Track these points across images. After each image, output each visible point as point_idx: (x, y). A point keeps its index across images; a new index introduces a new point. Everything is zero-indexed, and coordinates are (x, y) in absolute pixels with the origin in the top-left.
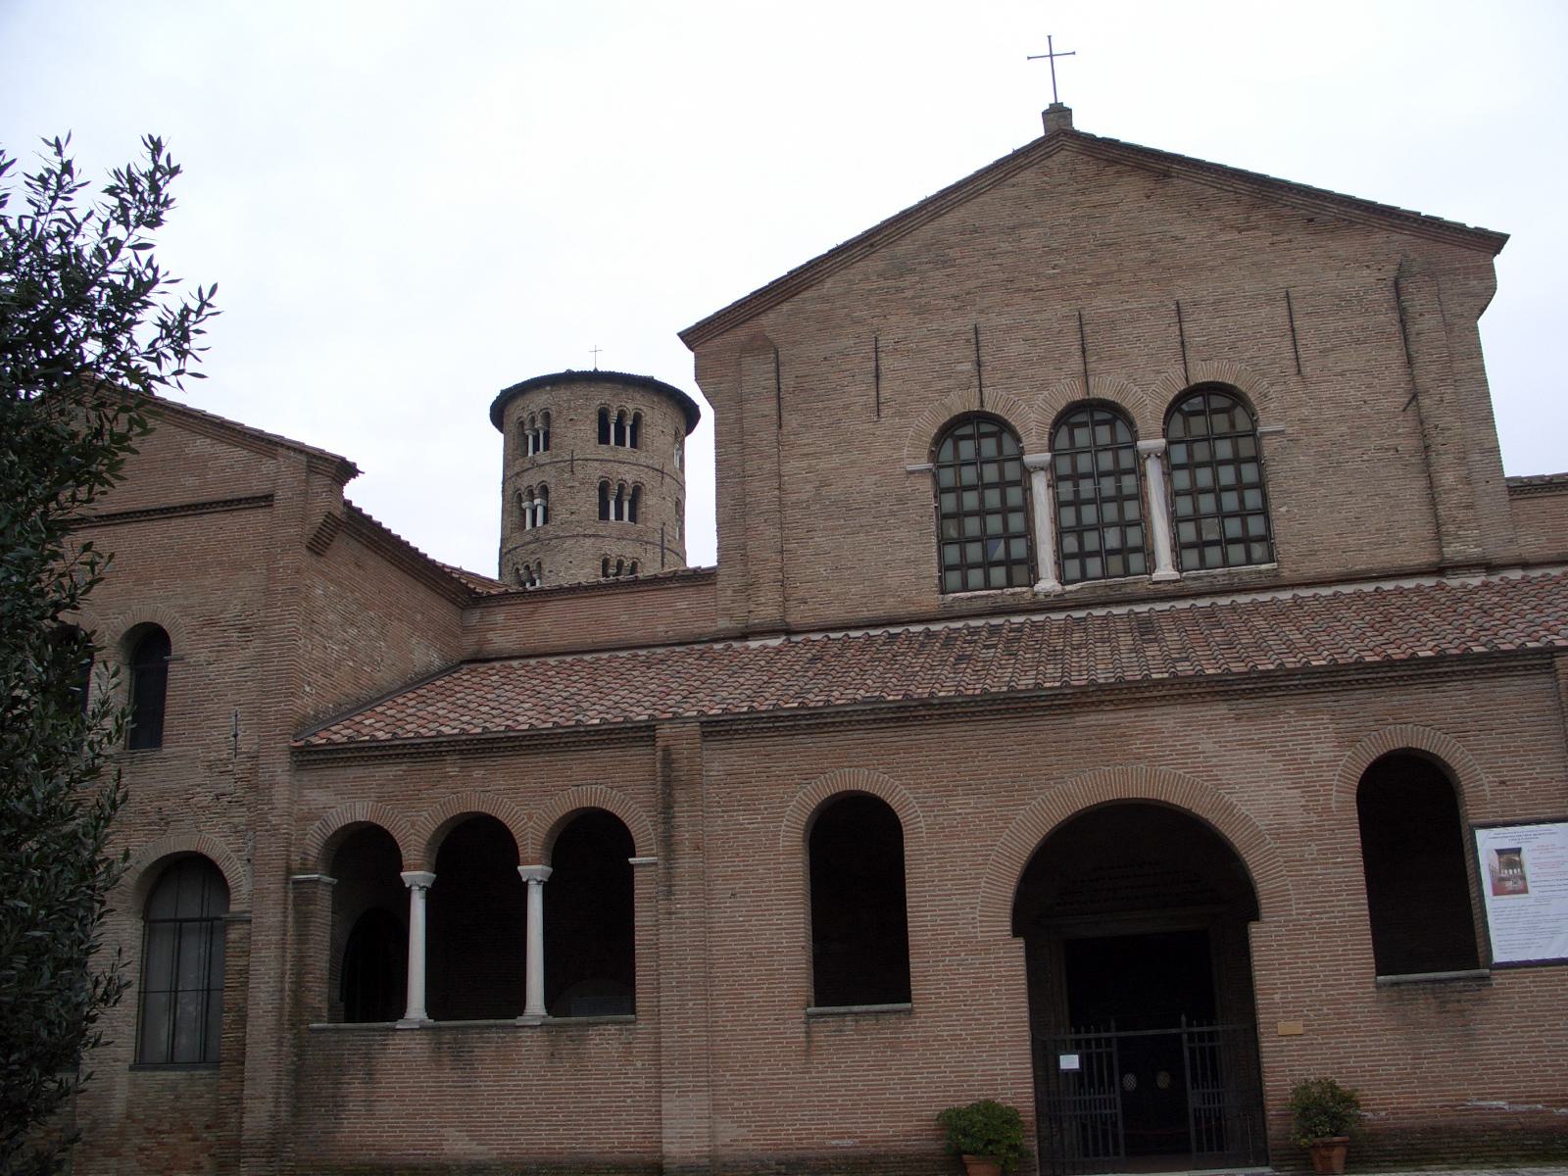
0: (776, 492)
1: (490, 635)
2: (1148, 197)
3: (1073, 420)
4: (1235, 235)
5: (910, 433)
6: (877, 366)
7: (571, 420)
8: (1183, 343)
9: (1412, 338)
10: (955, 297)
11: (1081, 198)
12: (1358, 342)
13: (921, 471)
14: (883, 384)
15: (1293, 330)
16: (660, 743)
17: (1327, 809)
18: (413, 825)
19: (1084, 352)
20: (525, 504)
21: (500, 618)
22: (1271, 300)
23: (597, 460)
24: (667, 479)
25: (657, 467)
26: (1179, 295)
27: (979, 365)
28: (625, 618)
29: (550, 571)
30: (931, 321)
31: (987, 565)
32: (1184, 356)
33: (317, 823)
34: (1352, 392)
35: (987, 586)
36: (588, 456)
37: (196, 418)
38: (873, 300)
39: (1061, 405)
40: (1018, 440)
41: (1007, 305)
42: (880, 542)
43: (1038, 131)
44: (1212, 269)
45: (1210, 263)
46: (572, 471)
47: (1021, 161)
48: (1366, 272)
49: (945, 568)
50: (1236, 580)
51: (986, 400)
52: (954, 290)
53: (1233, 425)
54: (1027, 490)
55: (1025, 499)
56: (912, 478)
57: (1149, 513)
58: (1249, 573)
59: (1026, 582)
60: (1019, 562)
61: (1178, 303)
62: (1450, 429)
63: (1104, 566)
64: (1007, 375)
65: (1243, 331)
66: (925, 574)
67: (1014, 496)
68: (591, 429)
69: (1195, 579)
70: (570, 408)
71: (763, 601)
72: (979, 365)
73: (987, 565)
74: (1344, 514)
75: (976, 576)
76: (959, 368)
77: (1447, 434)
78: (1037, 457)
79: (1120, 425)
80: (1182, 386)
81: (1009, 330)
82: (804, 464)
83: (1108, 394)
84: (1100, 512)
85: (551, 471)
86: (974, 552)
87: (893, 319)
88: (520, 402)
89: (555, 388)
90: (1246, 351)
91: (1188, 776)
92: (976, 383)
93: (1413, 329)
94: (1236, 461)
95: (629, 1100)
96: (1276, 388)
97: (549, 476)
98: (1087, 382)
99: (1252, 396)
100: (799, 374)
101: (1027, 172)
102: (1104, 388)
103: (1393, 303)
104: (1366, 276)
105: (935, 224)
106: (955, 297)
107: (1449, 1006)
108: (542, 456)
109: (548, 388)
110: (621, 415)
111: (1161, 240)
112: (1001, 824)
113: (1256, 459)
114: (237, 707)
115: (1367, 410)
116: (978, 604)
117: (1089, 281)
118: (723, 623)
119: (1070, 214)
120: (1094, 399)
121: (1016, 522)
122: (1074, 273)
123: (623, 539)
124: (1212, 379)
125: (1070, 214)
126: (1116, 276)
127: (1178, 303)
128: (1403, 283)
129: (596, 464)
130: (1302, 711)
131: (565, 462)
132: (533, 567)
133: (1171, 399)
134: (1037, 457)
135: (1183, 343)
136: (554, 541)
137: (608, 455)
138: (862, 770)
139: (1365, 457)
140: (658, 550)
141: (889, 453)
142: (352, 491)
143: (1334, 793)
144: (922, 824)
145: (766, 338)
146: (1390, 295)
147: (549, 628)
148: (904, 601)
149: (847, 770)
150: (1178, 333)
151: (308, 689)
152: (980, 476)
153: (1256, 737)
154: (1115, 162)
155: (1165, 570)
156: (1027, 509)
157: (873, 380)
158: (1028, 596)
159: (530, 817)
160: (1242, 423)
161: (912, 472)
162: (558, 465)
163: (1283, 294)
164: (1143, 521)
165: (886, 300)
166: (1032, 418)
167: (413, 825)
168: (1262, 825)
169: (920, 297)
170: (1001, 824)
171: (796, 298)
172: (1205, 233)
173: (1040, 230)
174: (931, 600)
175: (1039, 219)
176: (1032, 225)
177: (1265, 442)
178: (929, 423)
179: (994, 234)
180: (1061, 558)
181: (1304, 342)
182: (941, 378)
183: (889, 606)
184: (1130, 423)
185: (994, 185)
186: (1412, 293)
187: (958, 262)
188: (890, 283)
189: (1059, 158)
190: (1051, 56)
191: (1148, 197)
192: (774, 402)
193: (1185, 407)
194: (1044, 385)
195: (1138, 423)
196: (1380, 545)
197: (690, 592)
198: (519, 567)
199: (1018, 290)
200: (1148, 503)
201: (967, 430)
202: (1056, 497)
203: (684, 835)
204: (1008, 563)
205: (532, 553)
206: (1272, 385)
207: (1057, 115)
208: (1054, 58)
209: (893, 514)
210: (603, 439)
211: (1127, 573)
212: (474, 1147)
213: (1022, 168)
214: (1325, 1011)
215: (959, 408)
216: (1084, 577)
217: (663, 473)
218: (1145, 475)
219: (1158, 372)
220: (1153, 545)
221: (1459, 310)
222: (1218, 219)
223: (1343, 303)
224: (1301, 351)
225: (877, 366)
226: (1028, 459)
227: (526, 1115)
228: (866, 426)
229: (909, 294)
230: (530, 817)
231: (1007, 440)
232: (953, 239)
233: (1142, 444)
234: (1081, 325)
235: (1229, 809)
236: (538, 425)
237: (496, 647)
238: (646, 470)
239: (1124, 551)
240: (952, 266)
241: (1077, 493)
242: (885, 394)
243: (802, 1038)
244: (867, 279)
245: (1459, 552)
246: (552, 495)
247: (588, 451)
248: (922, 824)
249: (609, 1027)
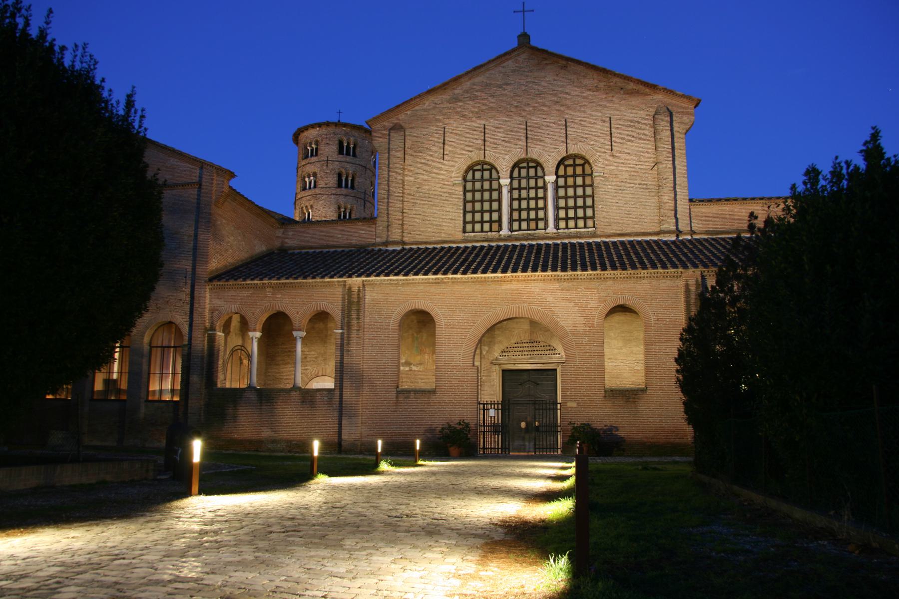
0: (401, 189)
1: (286, 240)
2: (557, 75)
3: (521, 165)
4: (591, 93)
5: (456, 168)
6: (444, 140)
7: (327, 144)
8: (566, 137)
9: (658, 140)
10: (477, 113)
11: (530, 74)
12: (636, 140)
13: (459, 184)
14: (446, 147)
15: (611, 134)
16: (347, 287)
17: (593, 325)
18: (253, 314)
19: (527, 138)
20: (307, 179)
21: (290, 234)
22: (603, 121)
24: (368, 171)
25: (363, 165)
26: (566, 117)
27: (485, 141)
28: (340, 236)
29: (316, 209)
30: (466, 122)
31: (482, 222)
32: (566, 142)
33: (217, 312)
34: (632, 161)
35: (482, 231)
36: (334, 160)
37: (171, 150)
38: (444, 112)
39: (516, 160)
40: (498, 173)
41: (497, 117)
42: (441, 210)
43: (516, 45)
44: (581, 107)
45: (580, 104)
46: (327, 166)
47: (507, 57)
48: (642, 112)
49: (465, 222)
50: (579, 234)
51: (486, 156)
52: (476, 110)
53: (583, 171)
54: (500, 193)
55: (499, 197)
56: (455, 186)
57: (547, 205)
58: (585, 232)
59: (497, 230)
60: (495, 221)
61: (566, 120)
62: (668, 178)
63: (528, 225)
64: (495, 146)
65: (591, 133)
66: (458, 225)
67: (495, 195)
68: (334, 148)
69: (563, 233)
70: (327, 138)
71: (394, 231)
72: (485, 141)
73: (482, 222)
74: (624, 210)
75: (478, 227)
76: (477, 142)
77: (667, 180)
78: (505, 182)
79: (539, 168)
80: (564, 154)
81: (497, 128)
82: (413, 178)
83: (535, 157)
84: (528, 203)
85: (318, 165)
86: (478, 217)
87: (452, 121)
88: (306, 134)
89: (321, 129)
90: (591, 141)
91: (542, 310)
92: (483, 148)
93: (658, 137)
94: (584, 186)
95: (330, 419)
96: (602, 157)
98: (527, 151)
99: (591, 161)
100: (414, 141)
101: (510, 61)
102: (534, 153)
103: (652, 125)
104: (642, 114)
105: (471, 81)
106: (477, 113)
107: (631, 400)
108: (314, 159)
110: (348, 144)
111: (561, 94)
112: (472, 324)
113: (592, 185)
114: (186, 267)
115: (637, 168)
116: (478, 238)
117: (531, 109)
118: (378, 240)
119: (525, 81)
120: (529, 158)
121: (495, 205)
122: (525, 106)
123: (348, 196)
124: (576, 152)
125: (525, 81)
126: (542, 108)
127: (566, 120)
128: (656, 116)
129: (337, 163)
130: (587, 289)
131: (324, 161)
133: (559, 159)
134: (505, 182)
135: (566, 137)
136: (319, 195)
137: (344, 159)
138: (422, 301)
139: (634, 188)
140: (362, 201)
141: (447, 175)
142: (234, 183)
143: (596, 319)
144: (443, 322)
145: (401, 125)
146: (651, 121)
147: (309, 239)
148: (449, 235)
149: (416, 301)
150: (565, 132)
151: (214, 260)
152: (482, 186)
153: (569, 297)
154: (546, 59)
155: (551, 229)
156: (499, 200)
157: (442, 145)
158: (497, 236)
159: (298, 313)
160: (588, 171)
161: (456, 184)
162: (321, 163)
163: (608, 119)
164: (545, 208)
165: (449, 112)
166: (504, 165)
167: (253, 314)
168: (568, 329)
169: (463, 112)
170: (472, 324)
171: (413, 109)
172: (579, 92)
173: (512, 87)
174: (460, 236)
175: (513, 82)
176: (511, 84)
177: (595, 179)
178: (462, 163)
179: (494, 87)
180: (511, 221)
181: (615, 139)
182: (469, 146)
183: (443, 236)
184: (543, 169)
185: (496, 66)
186: (659, 122)
187: (479, 98)
188: (452, 105)
189: (524, 56)
190: (524, 11)
191: (557, 75)
192: (402, 153)
193: (567, 162)
194: (508, 152)
195: (546, 170)
196: (637, 223)
197: (366, 227)
199: (502, 111)
200: (547, 201)
201: (479, 167)
202: (511, 196)
203: (354, 322)
204: (491, 222)
205: (309, 200)
206: (600, 156)
207: (524, 38)
208: (525, 13)
209: (447, 200)
210: (341, 152)
211: (537, 229)
212: (273, 434)
213: (507, 60)
214: (585, 399)
215: (475, 159)
216: (520, 229)
217: (366, 167)
218: (547, 189)
219: (555, 148)
220: (548, 218)
221: (678, 129)
222: (585, 86)
223: (632, 124)
224: (613, 143)
225: (444, 140)
226: (501, 181)
227: (293, 423)
228: (438, 164)
229: (459, 110)
230: (298, 313)
231: (494, 171)
232: (478, 88)
233: (547, 178)
234: (526, 127)
235: (557, 322)
237: (288, 245)
238: (359, 166)
239: (537, 219)
240: (478, 100)
241: (520, 195)
242: (446, 151)
243: (395, 399)
244: (442, 103)
245: (666, 228)
246: (318, 176)
247: (334, 157)
248: (443, 322)
249: (324, 392)
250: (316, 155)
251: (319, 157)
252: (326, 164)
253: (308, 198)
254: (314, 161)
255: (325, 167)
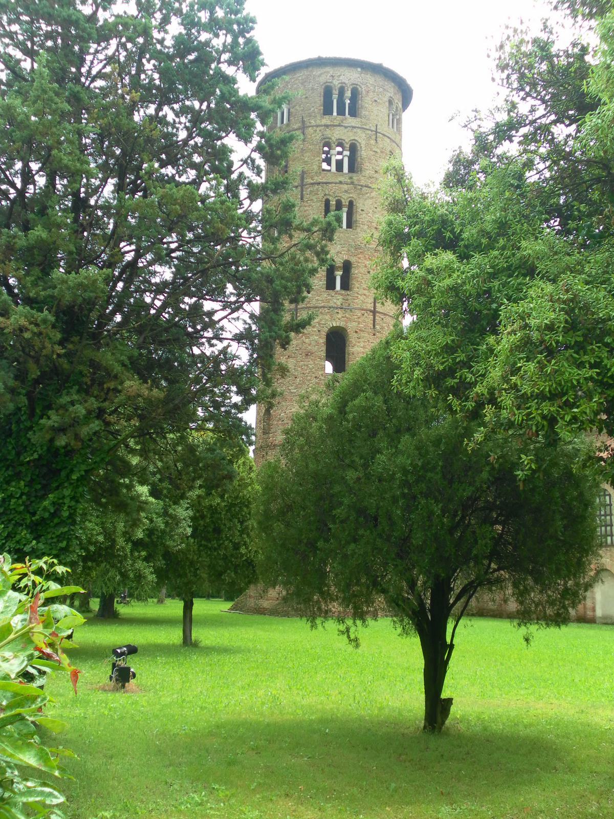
7: (376, 101)
23: (389, 138)
29: (362, 210)
97: (361, 138)
109: (359, 69)
129: (388, 140)
131: (372, 131)
132: (345, 202)
136: (364, 189)
198: (331, 198)
205: (346, 191)
236: (348, 94)
250: (354, 113)
251: (363, 120)
252: (374, 137)
253: (346, 187)
254: (353, 125)
255: (373, 142)
